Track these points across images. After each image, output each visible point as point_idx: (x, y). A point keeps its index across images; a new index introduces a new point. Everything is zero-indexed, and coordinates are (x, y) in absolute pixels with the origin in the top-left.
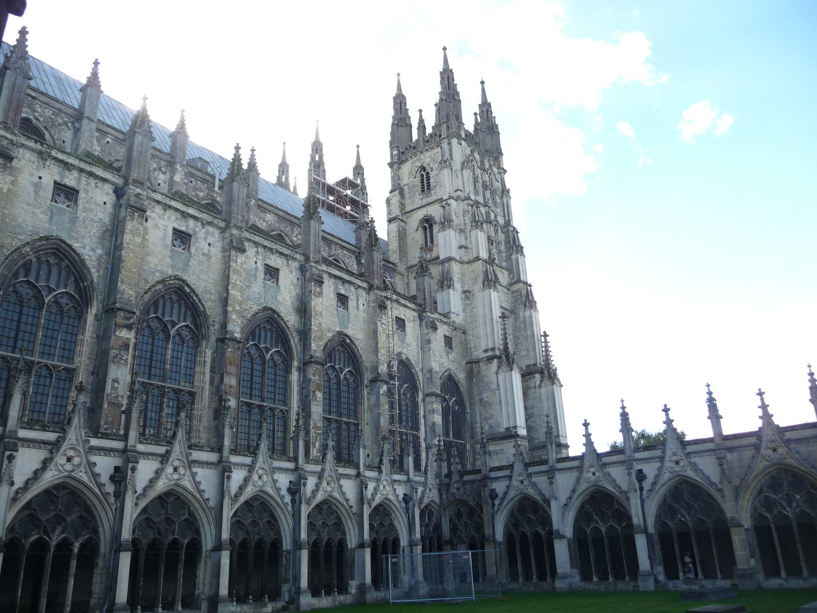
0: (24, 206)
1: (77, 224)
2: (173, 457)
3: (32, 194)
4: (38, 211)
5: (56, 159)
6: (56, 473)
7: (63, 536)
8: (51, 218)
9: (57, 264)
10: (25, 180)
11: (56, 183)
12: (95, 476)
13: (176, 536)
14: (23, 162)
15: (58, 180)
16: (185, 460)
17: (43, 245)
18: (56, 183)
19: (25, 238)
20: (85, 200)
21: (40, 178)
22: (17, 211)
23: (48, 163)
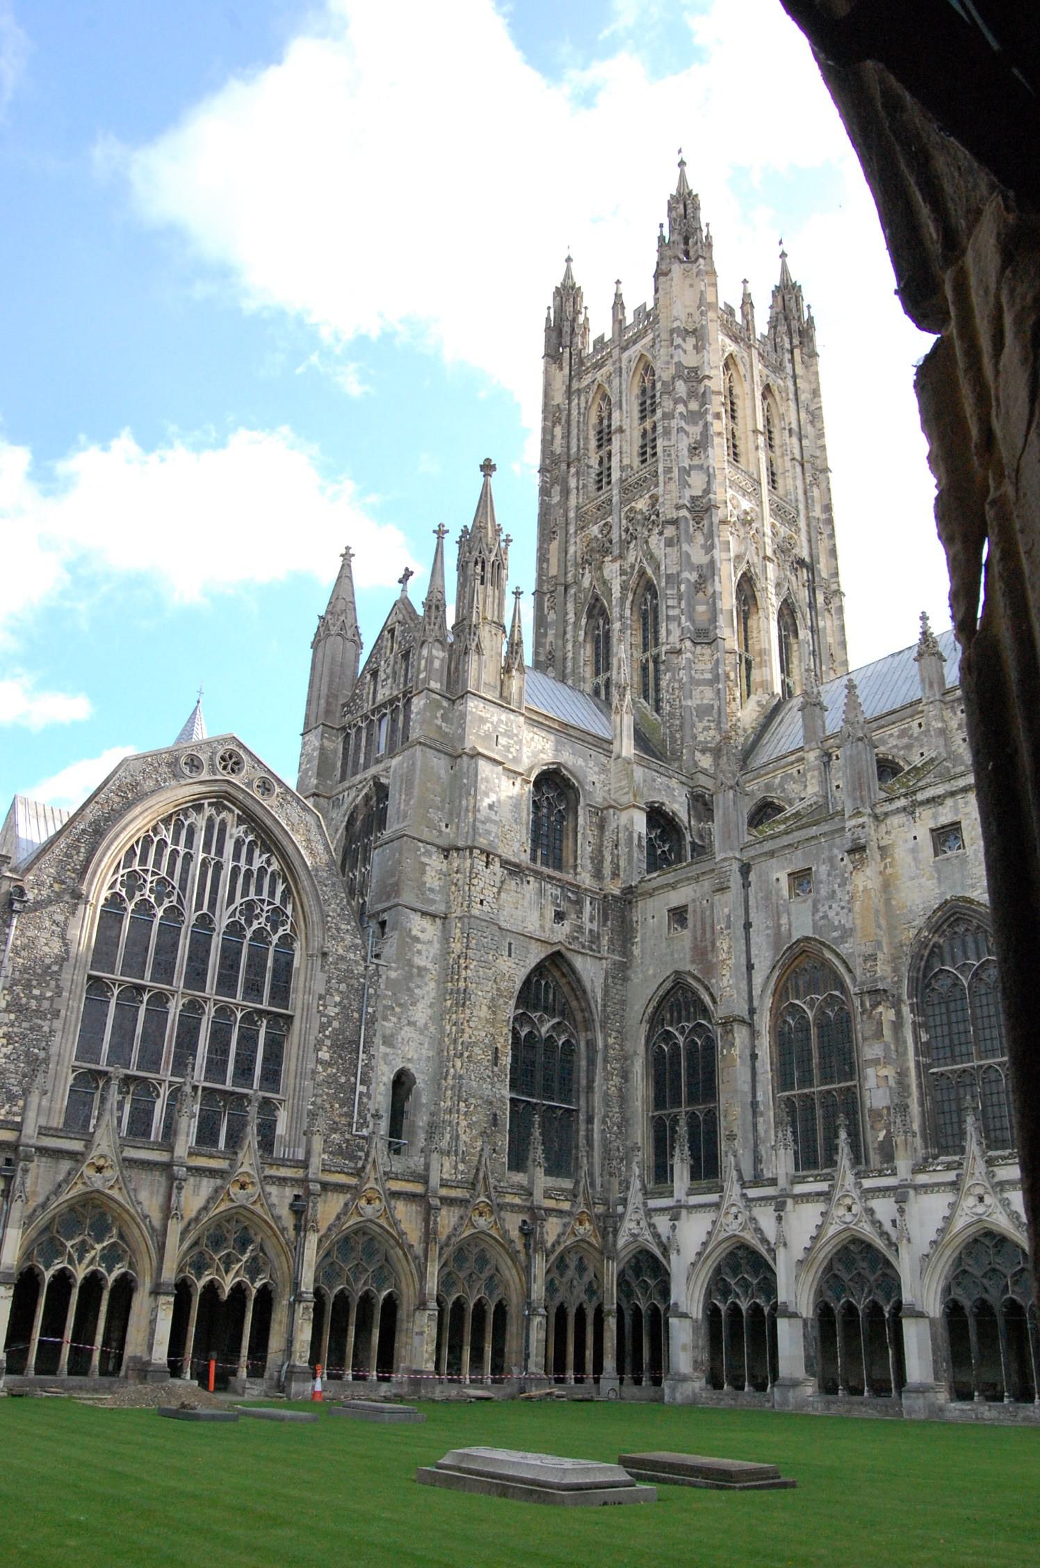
0: (909, 884)
1: (970, 866)
2: (969, 1182)
3: (913, 864)
4: (923, 880)
5: (922, 803)
6: (837, 1226)
7: (871, 1298)
8: (939, 879)
9: (967, 930)
10: (901, 854)
11: (932, 830)
12: (877, 1224)
13: (1010, 1295)
14: (894, 833)
15: (933, 826)
16: (987, 1185)
17: (940, 917)
18: (932, 830)
19: (919, 922)
20: (970, 828)
21: (915, 838)
22: (903, 895)
23: (917, 815)
